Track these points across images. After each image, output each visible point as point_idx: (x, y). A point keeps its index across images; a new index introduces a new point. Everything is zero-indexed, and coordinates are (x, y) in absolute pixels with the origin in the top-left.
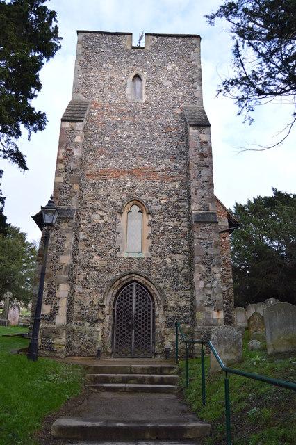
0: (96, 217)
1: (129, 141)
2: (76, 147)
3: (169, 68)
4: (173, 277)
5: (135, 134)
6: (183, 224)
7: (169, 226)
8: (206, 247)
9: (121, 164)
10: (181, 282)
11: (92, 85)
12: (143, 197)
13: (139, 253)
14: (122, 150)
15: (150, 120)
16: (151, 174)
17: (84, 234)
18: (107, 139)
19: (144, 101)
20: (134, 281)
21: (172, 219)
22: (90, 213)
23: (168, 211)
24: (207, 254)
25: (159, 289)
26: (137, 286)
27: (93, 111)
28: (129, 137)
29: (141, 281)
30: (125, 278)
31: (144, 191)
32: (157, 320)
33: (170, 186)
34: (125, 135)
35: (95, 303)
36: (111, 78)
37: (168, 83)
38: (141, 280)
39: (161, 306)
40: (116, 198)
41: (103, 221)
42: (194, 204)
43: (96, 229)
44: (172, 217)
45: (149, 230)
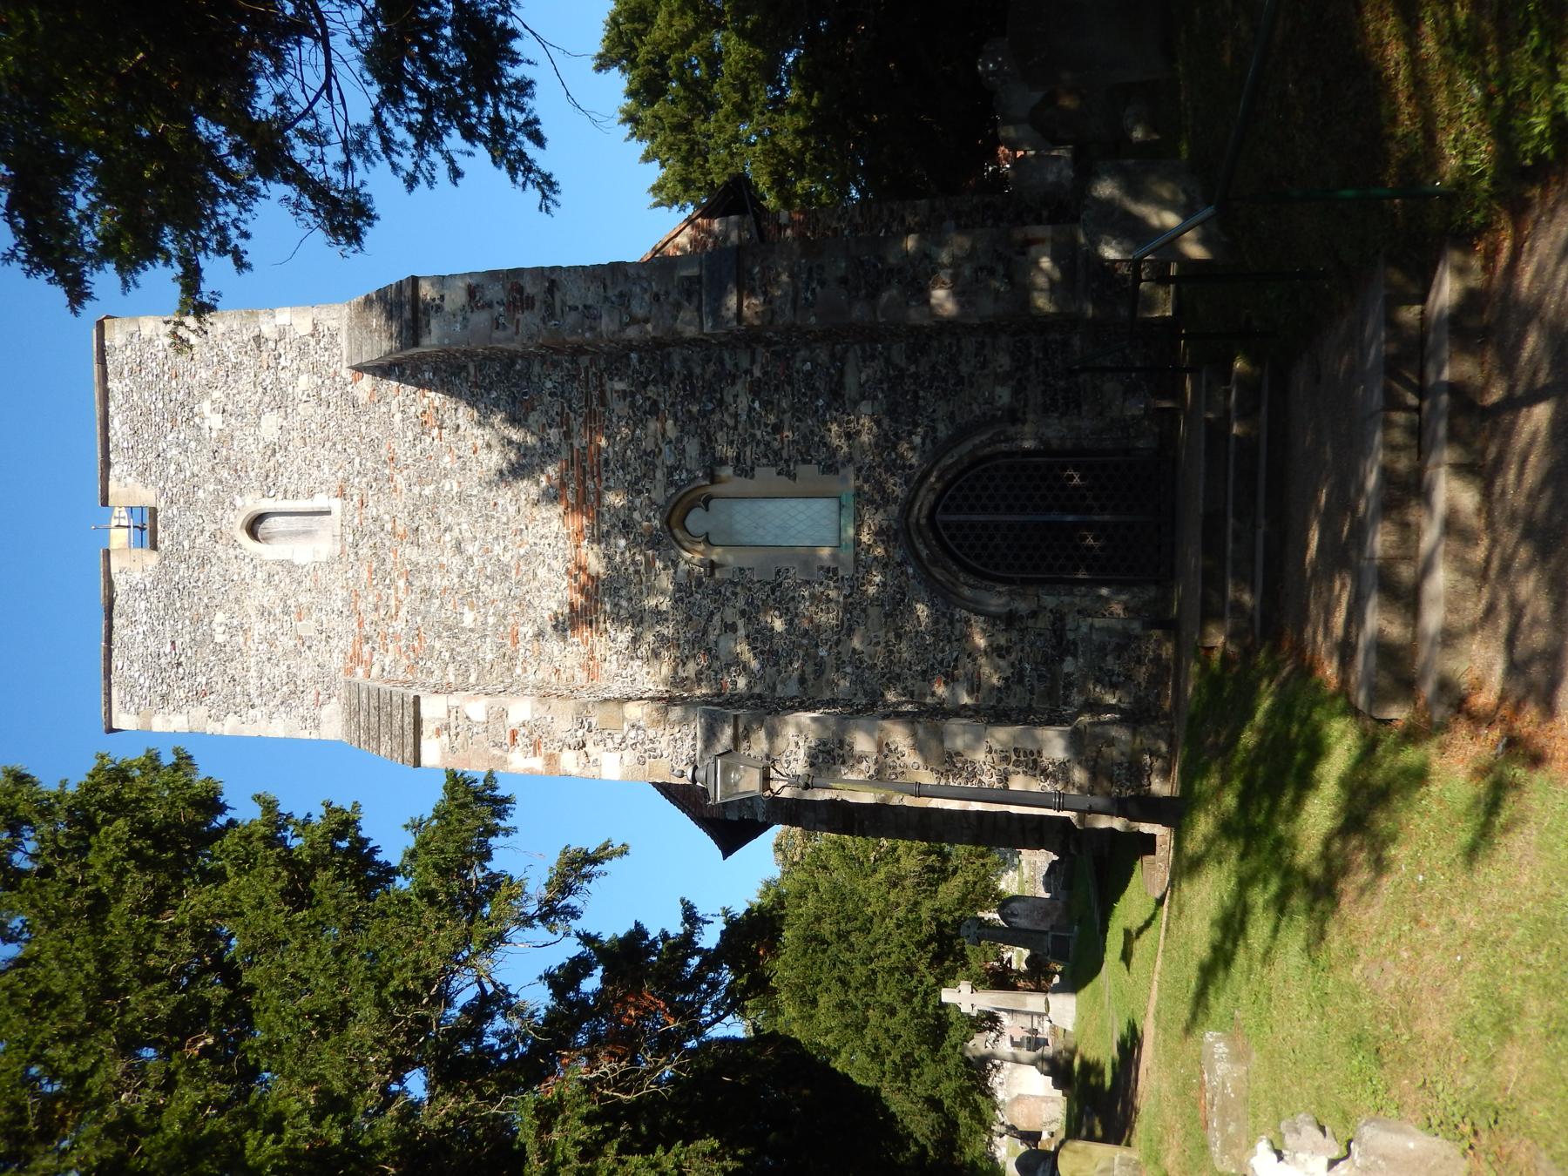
1: (471, 549)
2: (503, 714)
3: (216, 421)
4: (916, 393)
6: (745, 363)
7: (751, 409)
8: (822, 283)
9: (550, 569)
10: (933, 368)
11: (292, 678)
13: (841, 507)
14: (505, 572)
15: (400, 480)
17: (783, 682)
18: (469, 619)
19: (336, 505)
20: (931, 516)
21: (729, 399)
23: (704, 414)
24: (843, 281)
25: (962, 433)
26: (946, 509)
27: (375, 671)
28: (458, 547)
29: (932, 497)
30: (921, 547)
31: (640, 492)
32: (1055, 443)
34: (457, 562)
35: (1003, 641)
36: (263, 612)
37: (270, 424)
38: (925, 499)
39: (1011, 430)
41: (740, 623)
42: (679, 325)
44: (721, 402)
45: (766, 475)
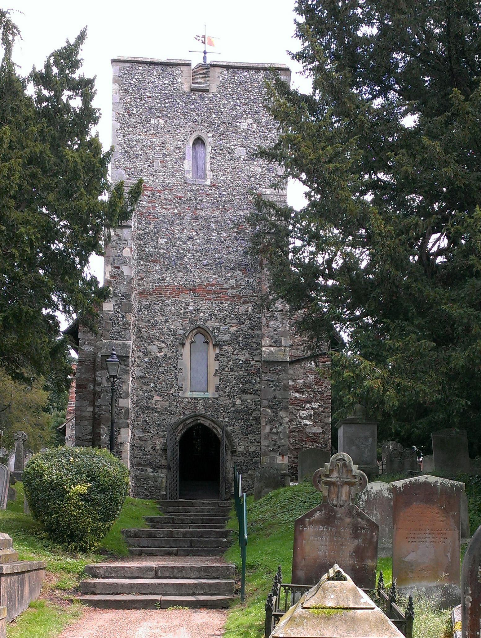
0: (153, 348)
5: (198, 234)
6: (256, 358)
7: (240, 360)
12: (209, 324)
15: (217, 213)
16: (218, 293)
17: (140, 370)
18: (162, 241)
22: (146, 344)
23: (238, 342)
28: (190, 238)
33: (242, 309)
34: (184, 236)
40: (176, 325)
41: (162, 354)
43: (154, 363)
